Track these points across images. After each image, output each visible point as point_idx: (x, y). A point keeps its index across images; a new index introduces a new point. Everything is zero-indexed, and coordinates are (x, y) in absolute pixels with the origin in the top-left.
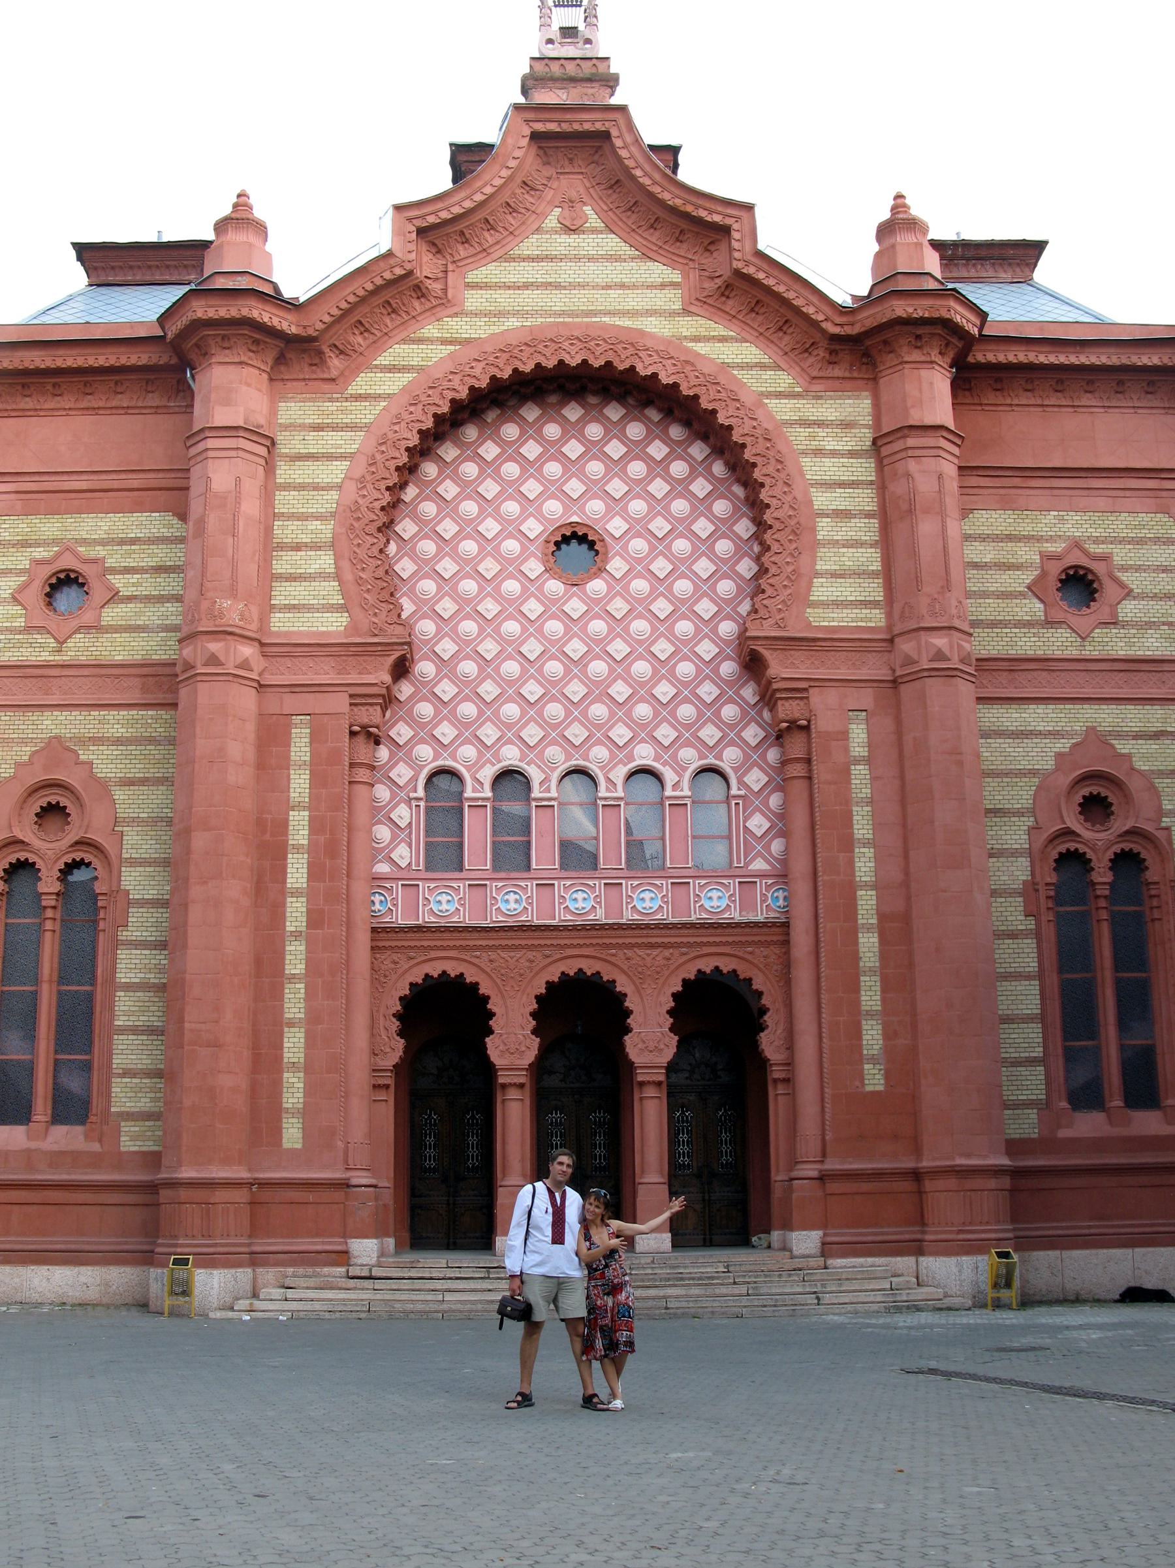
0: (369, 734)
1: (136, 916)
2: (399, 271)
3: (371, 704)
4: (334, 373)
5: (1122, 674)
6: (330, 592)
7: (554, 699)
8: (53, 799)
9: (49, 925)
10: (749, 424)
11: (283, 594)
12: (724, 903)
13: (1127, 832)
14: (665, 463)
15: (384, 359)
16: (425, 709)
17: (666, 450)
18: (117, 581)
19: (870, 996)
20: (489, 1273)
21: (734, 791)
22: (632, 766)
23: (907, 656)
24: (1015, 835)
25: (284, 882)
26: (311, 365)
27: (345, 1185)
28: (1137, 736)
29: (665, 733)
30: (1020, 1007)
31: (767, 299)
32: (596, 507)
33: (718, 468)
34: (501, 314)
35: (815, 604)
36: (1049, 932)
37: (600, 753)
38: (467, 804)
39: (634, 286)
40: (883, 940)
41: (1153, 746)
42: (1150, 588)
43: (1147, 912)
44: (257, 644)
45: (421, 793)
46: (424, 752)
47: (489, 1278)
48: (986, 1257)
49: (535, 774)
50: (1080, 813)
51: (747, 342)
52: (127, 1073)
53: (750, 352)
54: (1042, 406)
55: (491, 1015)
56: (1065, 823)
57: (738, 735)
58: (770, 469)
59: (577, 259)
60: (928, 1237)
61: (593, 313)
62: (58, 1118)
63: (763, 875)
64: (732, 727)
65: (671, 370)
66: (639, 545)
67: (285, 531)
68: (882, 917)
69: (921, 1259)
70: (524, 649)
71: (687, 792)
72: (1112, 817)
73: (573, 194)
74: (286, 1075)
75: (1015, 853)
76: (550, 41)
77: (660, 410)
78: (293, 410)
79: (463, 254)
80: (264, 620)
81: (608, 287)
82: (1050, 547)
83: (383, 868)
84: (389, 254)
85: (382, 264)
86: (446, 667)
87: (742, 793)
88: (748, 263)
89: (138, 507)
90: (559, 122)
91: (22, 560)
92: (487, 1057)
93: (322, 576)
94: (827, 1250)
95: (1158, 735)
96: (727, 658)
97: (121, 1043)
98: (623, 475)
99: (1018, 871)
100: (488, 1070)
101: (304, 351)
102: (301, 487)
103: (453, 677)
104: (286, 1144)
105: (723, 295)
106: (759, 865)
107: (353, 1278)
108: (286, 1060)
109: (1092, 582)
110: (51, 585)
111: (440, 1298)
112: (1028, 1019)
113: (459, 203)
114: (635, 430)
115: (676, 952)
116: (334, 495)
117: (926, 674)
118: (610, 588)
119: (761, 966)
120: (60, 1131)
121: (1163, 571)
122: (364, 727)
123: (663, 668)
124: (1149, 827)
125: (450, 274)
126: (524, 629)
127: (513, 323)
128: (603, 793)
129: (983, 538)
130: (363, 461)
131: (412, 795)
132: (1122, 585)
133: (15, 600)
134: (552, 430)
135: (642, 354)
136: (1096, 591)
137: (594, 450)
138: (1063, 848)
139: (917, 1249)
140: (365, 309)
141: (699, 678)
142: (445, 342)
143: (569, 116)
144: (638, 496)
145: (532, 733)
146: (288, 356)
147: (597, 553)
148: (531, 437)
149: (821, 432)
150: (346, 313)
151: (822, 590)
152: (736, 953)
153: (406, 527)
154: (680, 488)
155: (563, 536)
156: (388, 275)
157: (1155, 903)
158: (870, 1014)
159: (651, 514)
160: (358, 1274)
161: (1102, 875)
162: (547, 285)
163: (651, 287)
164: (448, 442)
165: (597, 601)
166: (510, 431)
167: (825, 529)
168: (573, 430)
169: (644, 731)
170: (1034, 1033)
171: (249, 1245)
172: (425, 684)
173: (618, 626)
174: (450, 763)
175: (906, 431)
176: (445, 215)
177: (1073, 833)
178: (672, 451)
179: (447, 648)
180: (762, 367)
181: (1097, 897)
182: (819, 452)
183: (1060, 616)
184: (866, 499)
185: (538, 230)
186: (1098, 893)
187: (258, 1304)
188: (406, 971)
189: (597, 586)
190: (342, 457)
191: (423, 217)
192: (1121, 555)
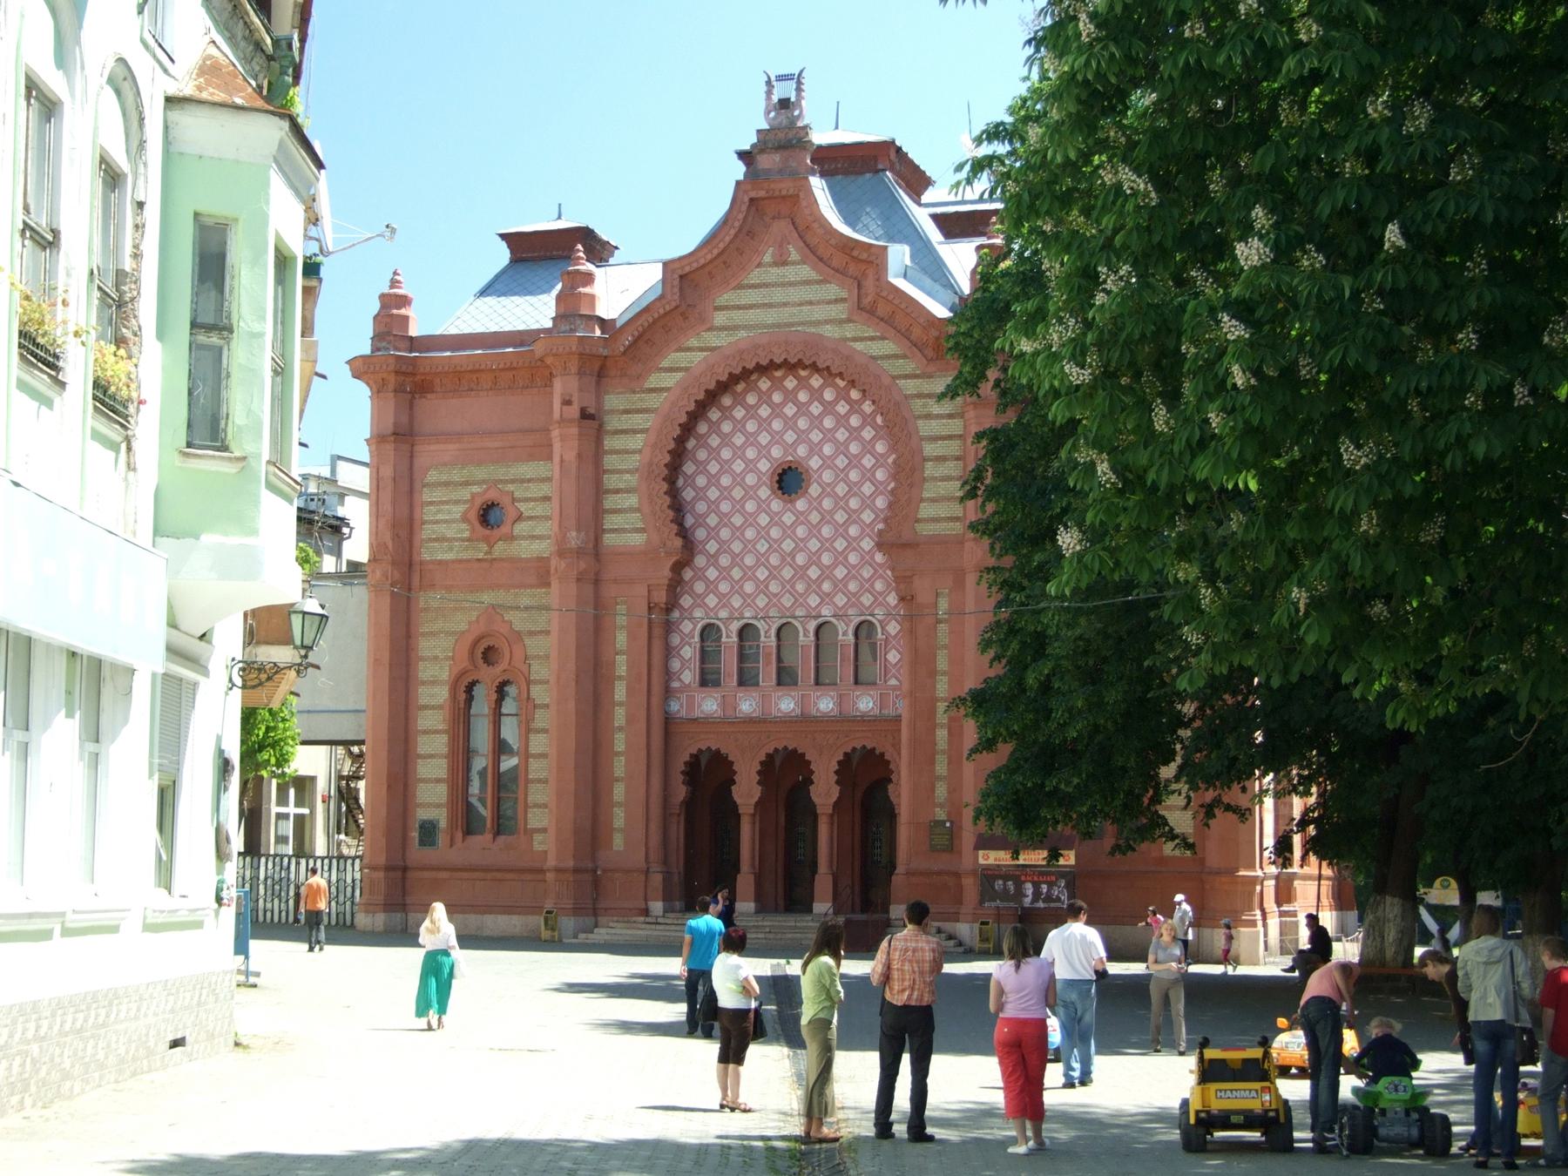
1: (539, 714)
2: (668, 308)
6: (635, 520)
7: (775, 577)
11: (611, 521)
15: (665, 364)
18: (522, 507)
19: (941, 768)
21: (879, 636)
22: (821, 620)
29: (840, 600)
32: (802, 451)
34: (736, 328)
35: (918, 521)
39: (819, 303)
40: (950, 734)
45: (697, 638)
46: (698, 613)
49: (760, 625)
52: (537, 806)
53: (888, 347)
55: (735, 773)
59: (783, 285)
61: (792, 325)
62: (498, 831)
63: (894, 688)
66: (827, 476)
67: (611, 481)
70: (758, 547)
71: (851, 637)
78: (613, 401)
80: (597, 540)
81: (801, 304)
84: (662, 297)
86: (713, 559)
89: (532, 457)
91: (465, 493)
93: (631, 510)
97: (533, 788)
100: (734, 807)
103: (716, 565)
106: (893, 682)
114: (828, 395)
116: (637, 457)
118: (810, 503)
120: (501, 839)
123: (841, 559)
126: (759, 533)
127: (743, 334)
133: (465, 519)
134: (777, 397)
137: (802, 409)
139: (955, 918)
142: (701, 349)
145: (761, 601)
150: (640, 336)
151: (926, 511)
153: (689, 468)
154: (855, 434)
156: (662, 311)
158: (939, 778)
163: (829, 302)
164: (714, 409)
165: (802, 513)
166: (751, 399)
167: (930, 469)
168: (790, 396)
169: (826, 598)
172: (700, 569)
173: (814, 530)
176: (695, 265)
178: (852, 407)
179: (712, 547)
180: (896, 357)
182: (928, 416)
185: (759, 265)
187: (590, 936)
189: (801, 504)
191: (683, 268)
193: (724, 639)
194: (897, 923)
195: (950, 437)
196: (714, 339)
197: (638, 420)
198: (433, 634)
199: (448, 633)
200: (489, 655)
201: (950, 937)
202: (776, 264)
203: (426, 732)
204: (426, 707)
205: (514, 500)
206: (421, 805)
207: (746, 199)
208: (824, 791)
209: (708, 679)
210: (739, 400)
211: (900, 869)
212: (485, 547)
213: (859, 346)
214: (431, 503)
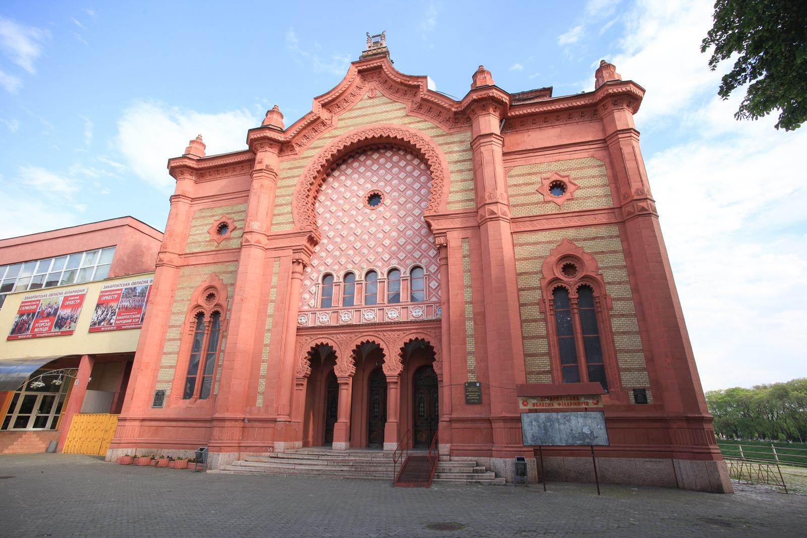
0: (299, 263)
2: (315, 117)
3: (299, 252)
4: (297, 152)
5: (577, 217)
8: (211, 292)
9: (206, 332)
10: (427, 146)
12: (420, 314)
13: (583, 277)
14: (405, 166)
16: (323, 254)
17: (405, 163)
19: (470, 346)
20: (319, 457)
23: (481, 215)
24: (535, 281)
25: (267, 313)
26: (291, 151)
27: (275, 421)
28: (585, 240)
30: (540, 350)
31: (433, 106)
33: (423, 166)
34: (349, 126)
35: (448, 203)
36: (551, 319)
37: (380, 264)
38: (334, 284)
39: (391, 111)
40: (475, 324)
41: (592, 243)
42: (587, 184)
43: (596, 309)
44: (264, 235)
45: (320, 281)
47: (318, 459)
48: (514, 459)
49: (357, 272)
50: (563, 271)
51: (427, 121)
53: (429, 124)
54: (540, 128)
56: (555, 275)
57: (427, 254)
58: (434, 160)
60: (494, 449)
61: (377, 121)
63: (435, 303)
64: (425, 251)
65: (401, 134)
66: (395, 194)
68: (475, 314)
69: (492, 458)
71: (408, 275)
72: (577, 272)
73: (373, 88)
74: (260, 380)
75: (534, 289)
76: (370, 47)
77: (403, 151)
78: (286, 165)
79: (338, 110)
80: (268, 229)
82: (545, 175)
83: (306, 308)
84: (312, 112)
85: (310, 116)
87: (428, 274)
88: (425, 95)
90: (366, 65)
91: (211, 220)
92: (334, 373)
93: (288, 213)
94: (451, 453)
95: (594, 239)
96: (424, 228)
98: (391, 173)
99: (537, 295)
101: (288, 146)
102: (284, 187)
104: (258, 405)
105: (419, 108)
106: (434, 299)
107: (271, 457)
108: (261, 374)
109: (563, 185)
110: (219, 227)
111: (294, 467)
112: (543, 355)
113: (334, 94)
114: (395, 158)
115: (401, 332)
117: (489, 220)
118: (385, 209)
119: (433, 337)
120: (199, 401)
121: (592, 178)
122: (297, 260)
124: (593, 274)
125: (333, 117)
128: (379, 277)
129: (519, 176)
130: (302, 177)
131: (317, 283)
132: (575, 185)
134: (369, 162)
135: (392, 131)
136: (565, 188)
137: (382, 166)
138: (556, 286)
140: (306, 131)
141: (414, 235)
142: (330, 137)
143: (369, 63)
144: (396, 179)
146: (284, 148)
147: (381, 198)
148: (362, 165)
149: (452, 146)
150: (299, 133)
152: (424, 332)
153: (321, 198)
155: (371, 195)
156: (312, 119)
157: (598, 305)
158: (470, 353)
159: (400, 184)
160: (273, 456)
161: (573, 294)
162: (363, 116)
163: (397, 110)
164: (337, 171)
166: (356, 164)
168: (376, 161)
170: (546, 360)
171: (240, 443)
174: (329, 271)
175: (479, 137)
176: (330, 99)
177: (560, 279)
179: (331, 234)
181: (572, 304)
183: (550, 199)
184: (468, 165)
185: (361, 100)
186: (572, 302)
188: (310, 343)
189: (381, 208)
190: (297, 176)
192: (573, 174)
193: (335, 280)
194: (445, 458)
195: (465, 161)
196: (336, 132)
197: (295, 172)
198: (183, 288)
199: (191, 288)
200: (211, 296)
201: (487, 470)
202: (371, 98)
203: (170, 340)
204: (172, 326)
205: (234, 221)
206: (159, 382)
207: (357, 70)
208: (392, 366)
209: (326, 303)
210: (350, 166)
211: (446, 418)
212: (216, 244)
213: (412, 126)
214: (195, 226)
